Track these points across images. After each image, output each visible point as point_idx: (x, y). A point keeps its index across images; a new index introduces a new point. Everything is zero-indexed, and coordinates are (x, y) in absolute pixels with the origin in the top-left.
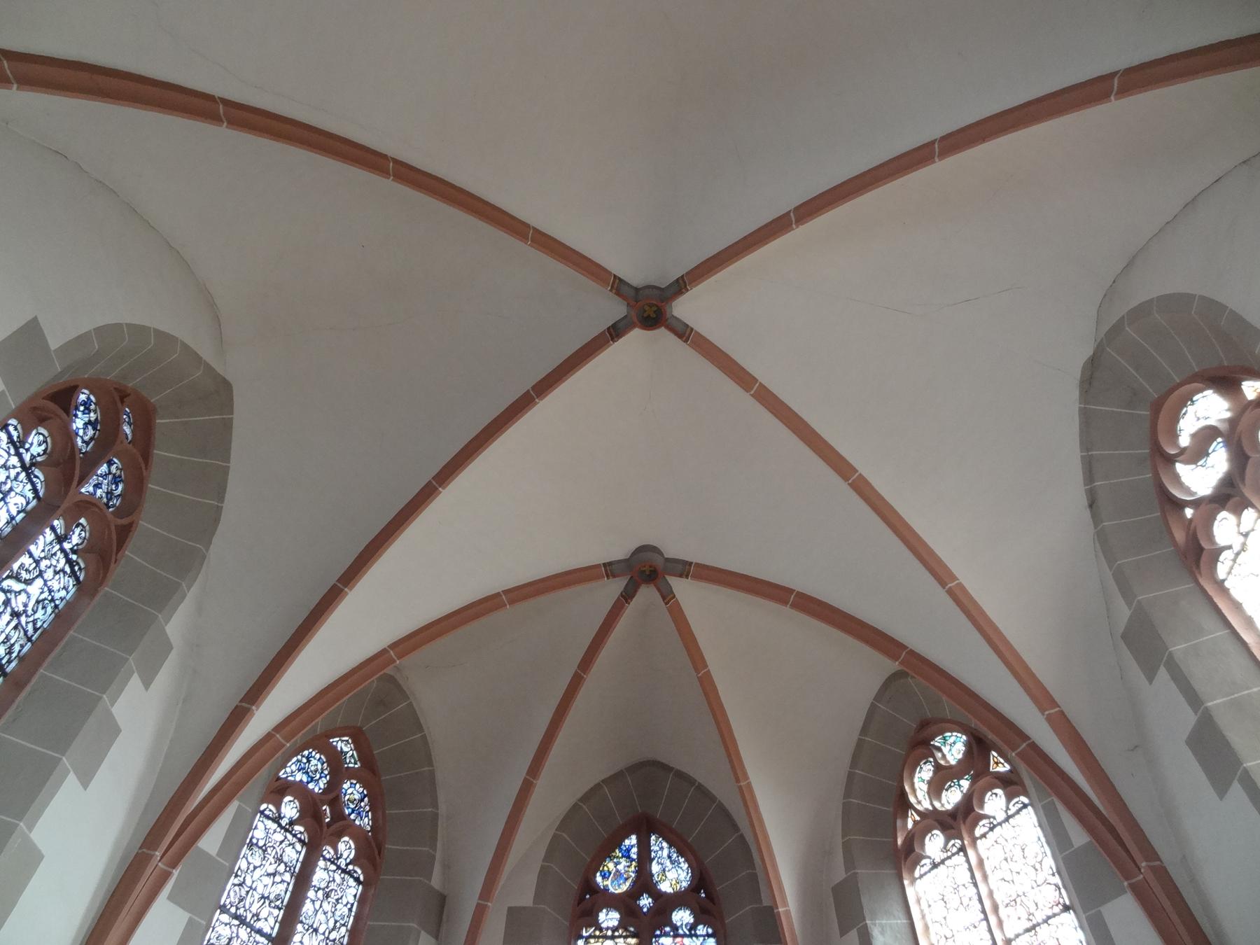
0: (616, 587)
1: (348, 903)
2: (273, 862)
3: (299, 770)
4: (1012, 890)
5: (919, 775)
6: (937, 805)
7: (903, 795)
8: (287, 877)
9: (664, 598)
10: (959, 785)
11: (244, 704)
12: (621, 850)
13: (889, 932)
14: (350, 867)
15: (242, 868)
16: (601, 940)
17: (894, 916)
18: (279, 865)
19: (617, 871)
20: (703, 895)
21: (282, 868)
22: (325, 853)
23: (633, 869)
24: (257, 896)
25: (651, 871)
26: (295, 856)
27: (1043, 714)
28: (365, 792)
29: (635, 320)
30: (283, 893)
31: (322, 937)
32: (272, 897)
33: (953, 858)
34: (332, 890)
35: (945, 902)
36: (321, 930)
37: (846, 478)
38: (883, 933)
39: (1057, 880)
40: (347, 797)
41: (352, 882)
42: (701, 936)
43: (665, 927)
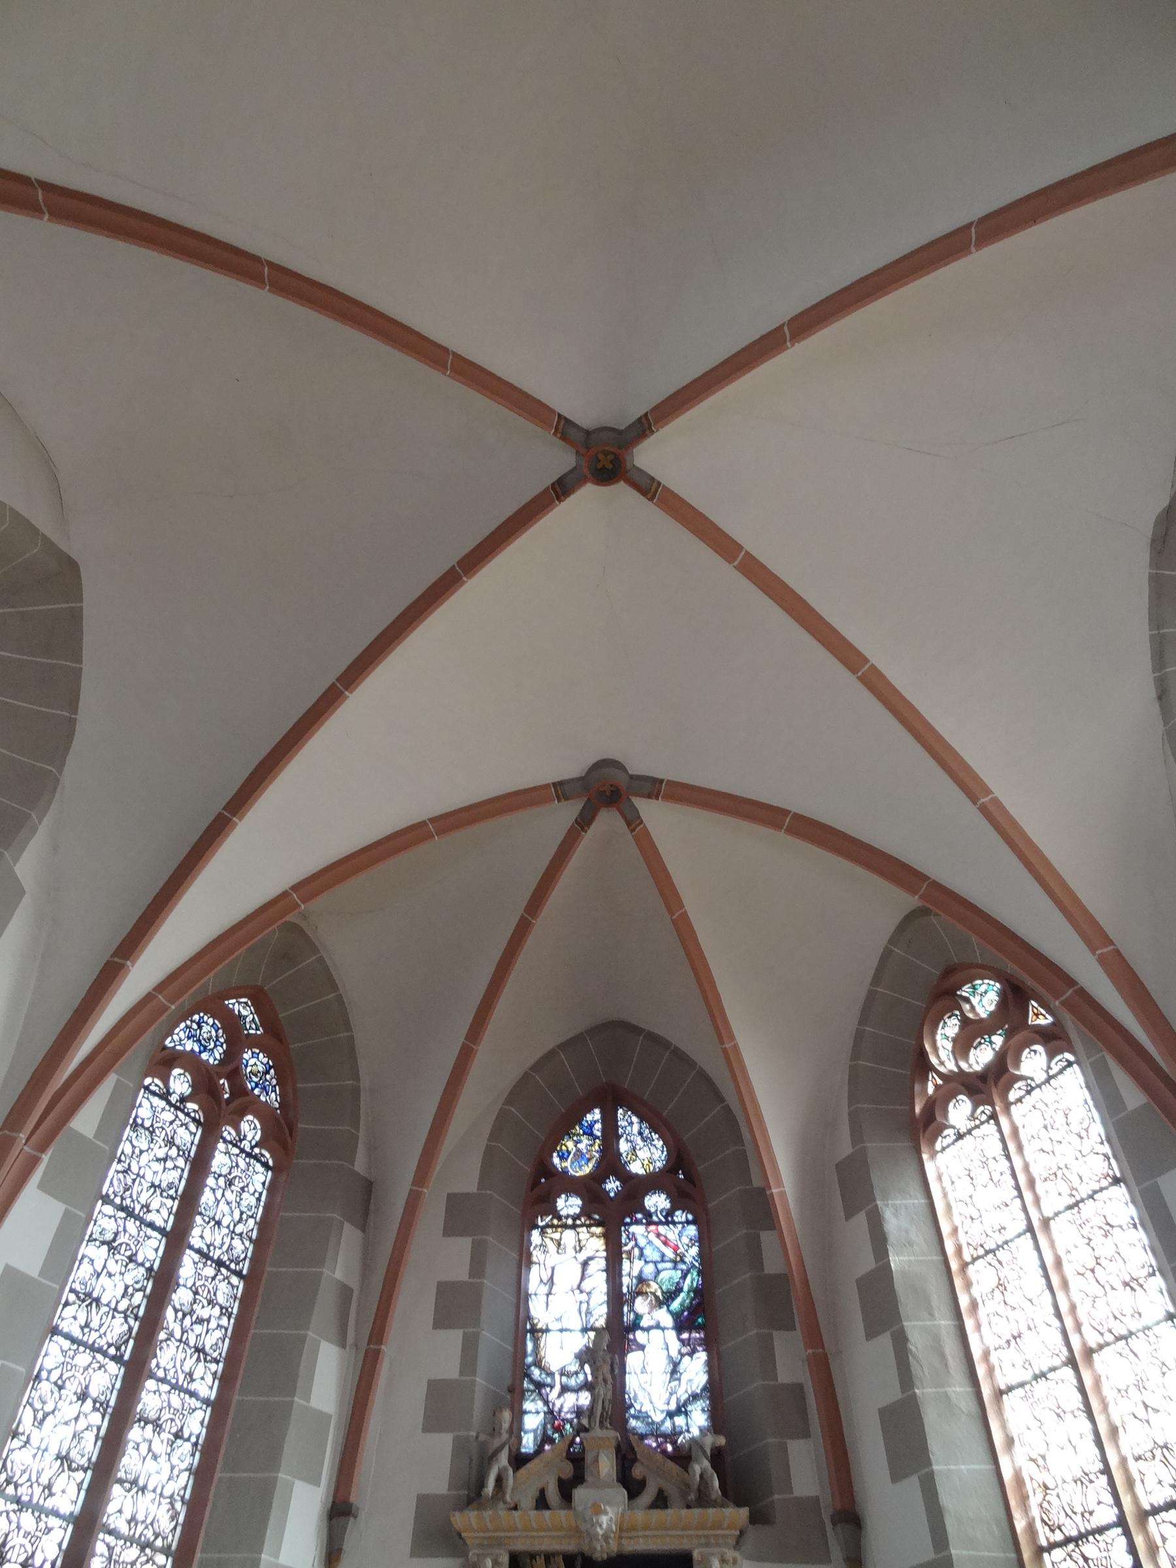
0: (567, 812)
1: (255, 1191)
2: (163, 1145)
3: (189, 1038)
4: (1050, 1162)
5: (943, 1031)
6: (964, 1065)
7: (923, 1054)
8: (181, 1162)
10: (991, 1042)
11: (116, 959)
12: (581, 1127)
13: (903, 1213)
14: (257, 1150)
15: (126, 1152)
16: (559, 1230)
17: (910, 1196)
18: (170, 1148)
19: (578, 1150)
20: (681, 1176)
21: (174, 1152)
22: (225, 1134)
23: (597, 1147)
24: (146, 1185)
25: (618, 1149)
26: (188, 1138)
27: (1094, 954)
28: (271, 1063)
29: (586, 471)
30: (177, 1181)
31: (226, 1231)
32: (164, 1185)
33: (981, 1127)
34: (235, 1177)
35: (972, 1179)
36: (225, 1222)
37: (854, 671)
38: (896, 1216)
39: (1106, 1149)
40: (249, 1069)
41: (258, 1167)
42: (679, 1223)
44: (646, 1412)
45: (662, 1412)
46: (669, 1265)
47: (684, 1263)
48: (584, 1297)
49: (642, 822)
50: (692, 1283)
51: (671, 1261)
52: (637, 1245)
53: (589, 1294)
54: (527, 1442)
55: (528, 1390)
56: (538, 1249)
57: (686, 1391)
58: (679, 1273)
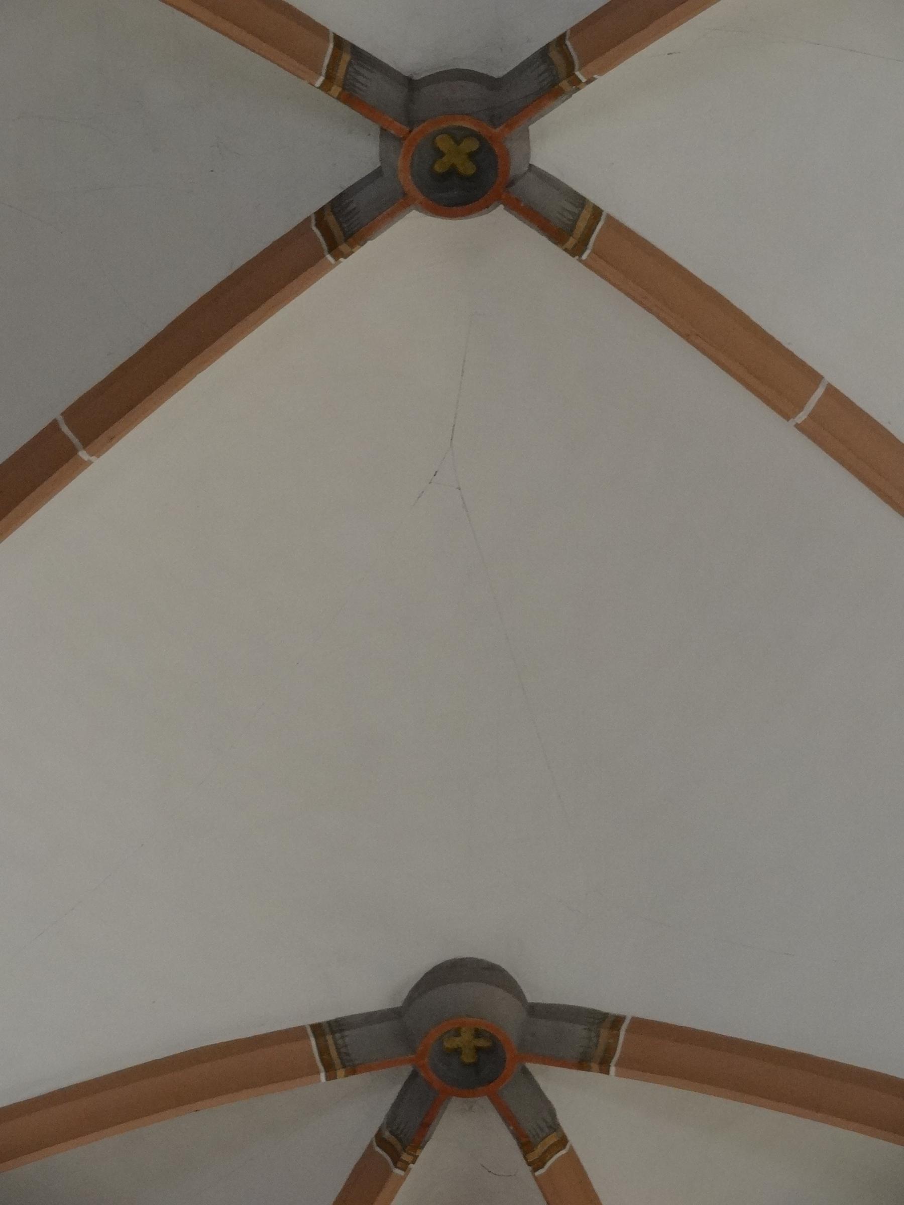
9: (526, 1145)
29: (406, 180)
49: (563, 1141)
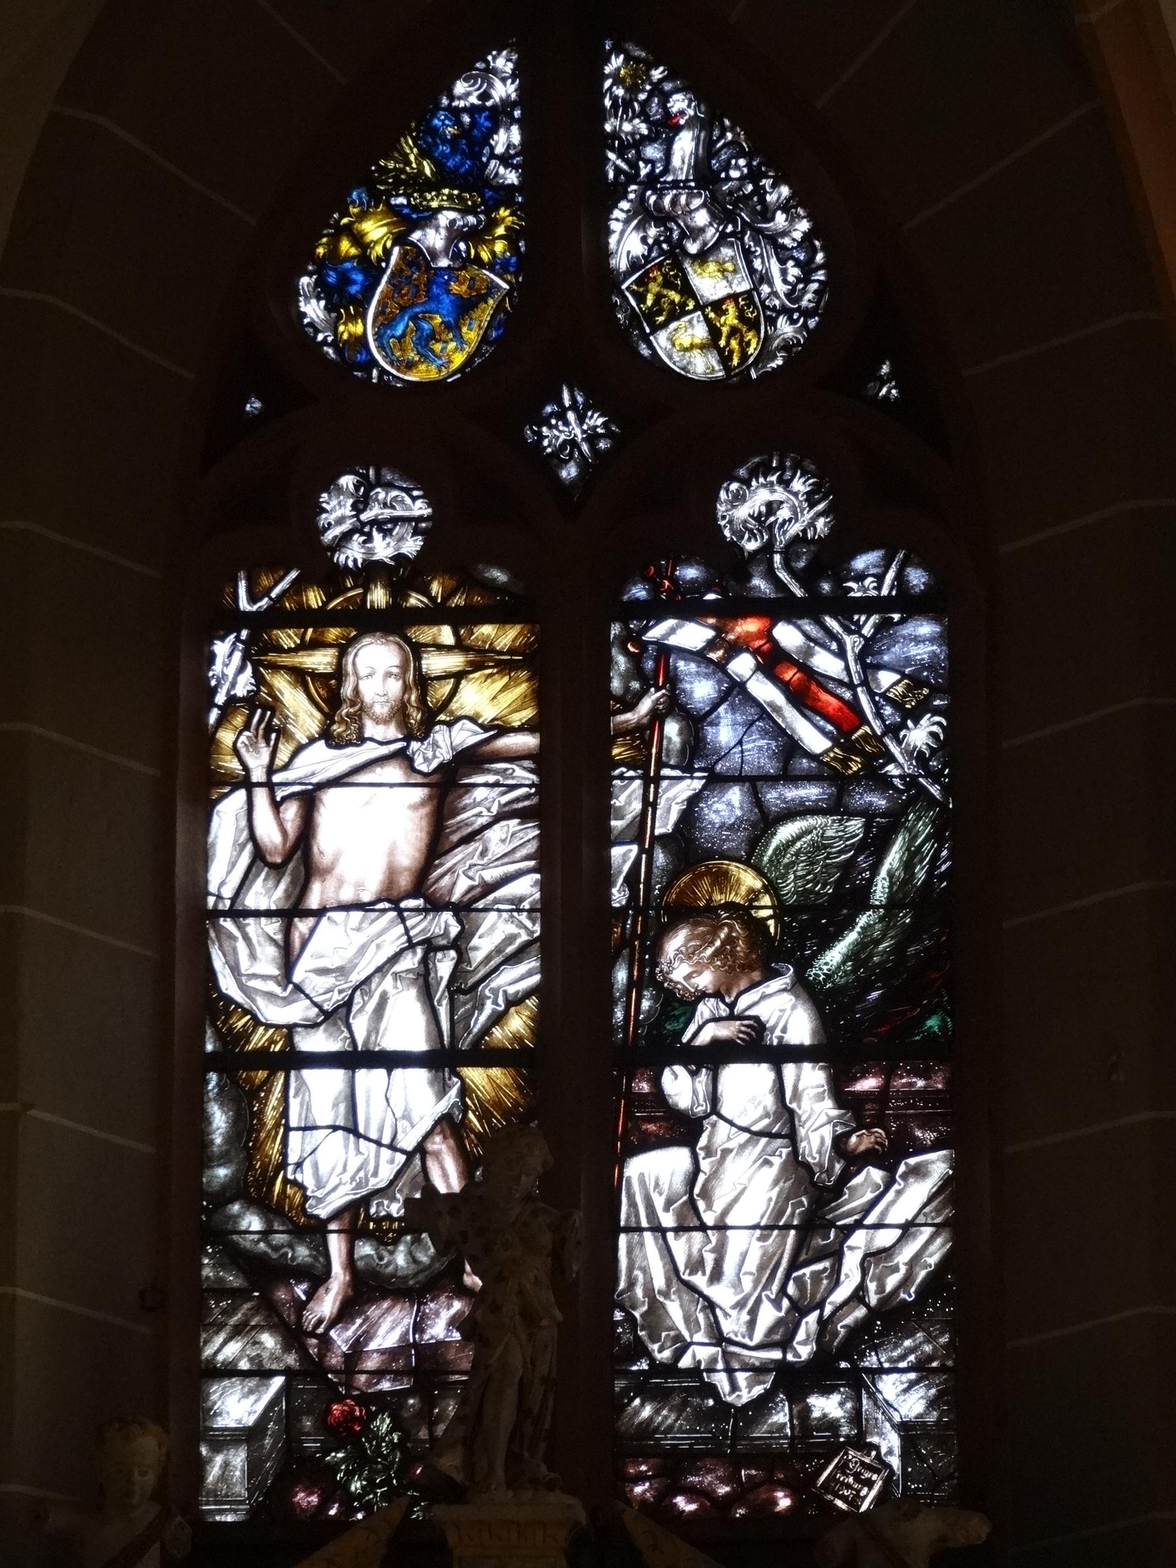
16: (333, 633)
19: (417, 258)
42: (869, 605)
43: (679, 561)
44: (695, 1372)
45: (759, 1370)
46: (811, 792)
47: (885, 783)
48: (447, 923)
50: (908, 865)
51: (822, 771)
52: (675, 705)
53: (464, 909)
54: (223, 1477)
55: (221, 1291)
56: (239, 721)
57: (859, 1295)
58: (855, 825)
